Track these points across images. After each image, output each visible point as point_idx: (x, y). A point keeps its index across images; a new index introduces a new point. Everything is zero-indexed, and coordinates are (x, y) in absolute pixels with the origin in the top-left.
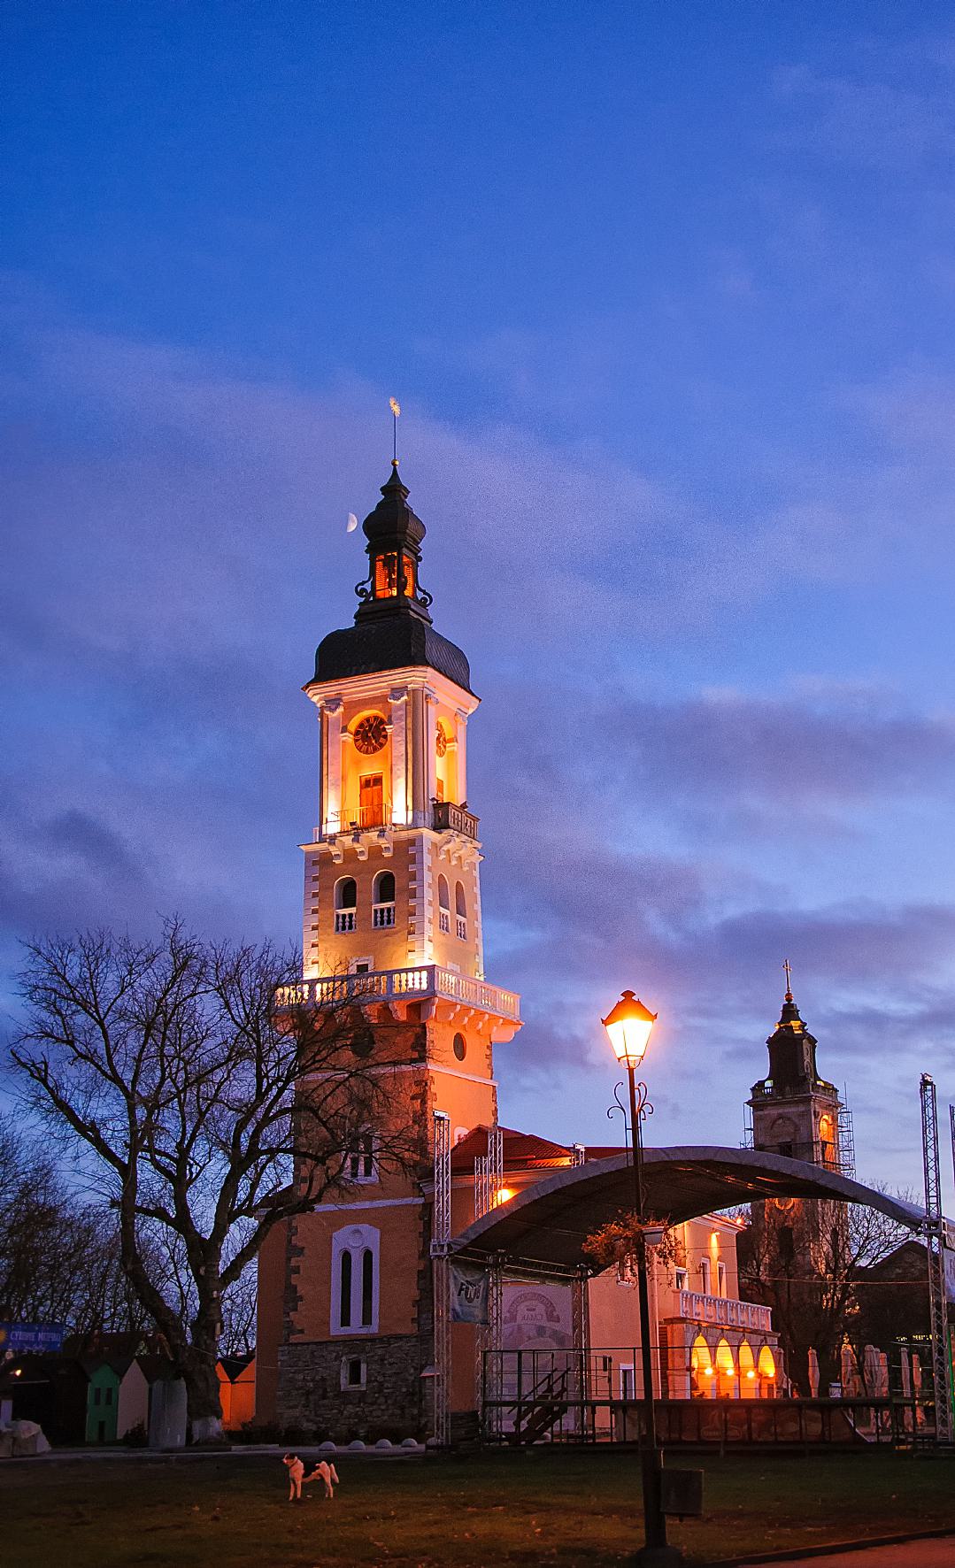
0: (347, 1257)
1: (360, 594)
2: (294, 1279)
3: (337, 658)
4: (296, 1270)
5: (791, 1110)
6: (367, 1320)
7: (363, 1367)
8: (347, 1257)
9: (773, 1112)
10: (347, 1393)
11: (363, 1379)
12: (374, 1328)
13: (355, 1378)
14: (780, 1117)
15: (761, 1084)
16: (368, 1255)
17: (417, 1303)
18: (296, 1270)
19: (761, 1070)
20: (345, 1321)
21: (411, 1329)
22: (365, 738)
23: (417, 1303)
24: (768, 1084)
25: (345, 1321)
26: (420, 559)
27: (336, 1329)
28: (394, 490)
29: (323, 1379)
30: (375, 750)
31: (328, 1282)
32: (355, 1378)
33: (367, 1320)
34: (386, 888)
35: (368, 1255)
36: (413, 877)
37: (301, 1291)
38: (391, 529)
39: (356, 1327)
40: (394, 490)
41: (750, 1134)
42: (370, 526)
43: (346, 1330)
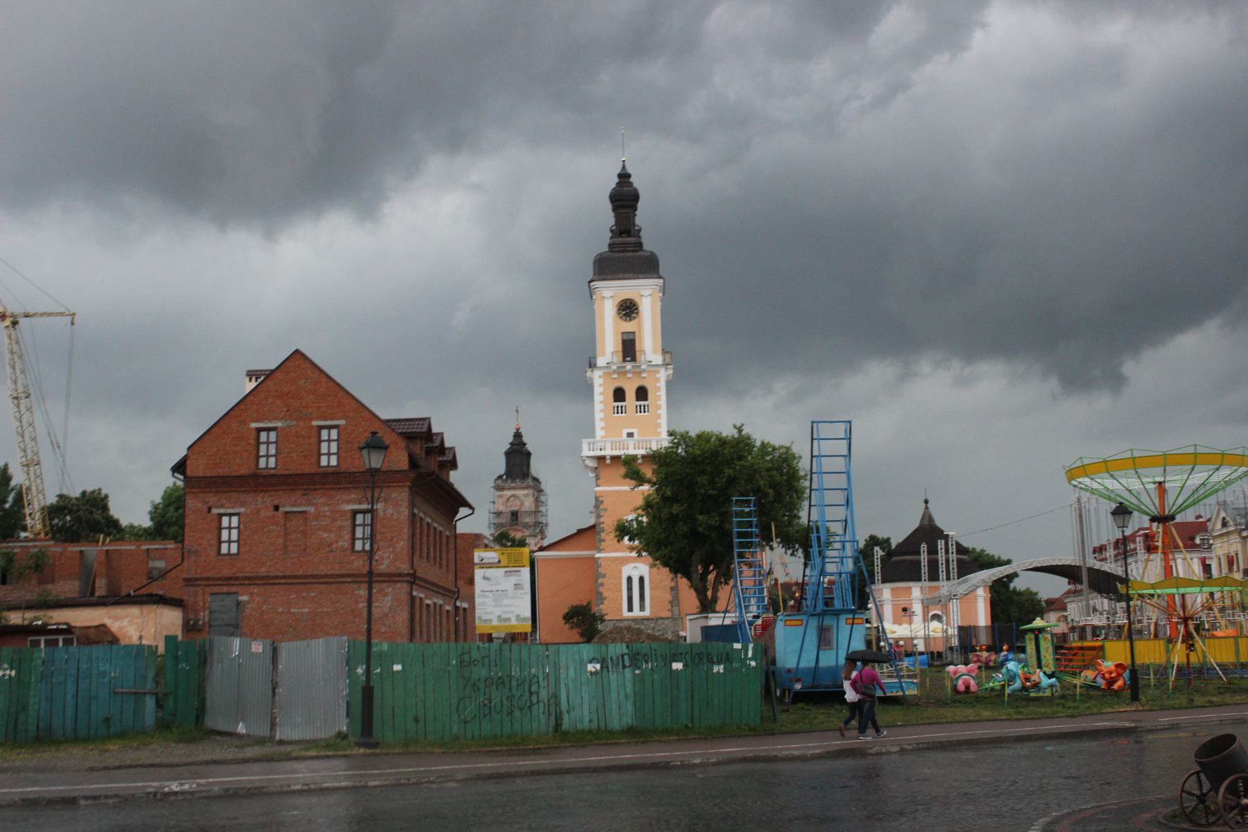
0: (630, 579)
2: (601, 589)
4: (602, 585)
6: (642, 608)
8: (630, 579)
9: (509, 493)
12: (647, 613)
16: (641, 579)
17: (671, 602)
18: (602, 585)
20: (630, 609)
21: (669, 614)
23: (671, 602)
25: (630, 609)
27: (626, 614)
31: (620, 591)
33: (642, 608)
34: (642, 393)
35: (641, 579)
37: (605, 594)
39: (636, 613)
43: (630, 614)
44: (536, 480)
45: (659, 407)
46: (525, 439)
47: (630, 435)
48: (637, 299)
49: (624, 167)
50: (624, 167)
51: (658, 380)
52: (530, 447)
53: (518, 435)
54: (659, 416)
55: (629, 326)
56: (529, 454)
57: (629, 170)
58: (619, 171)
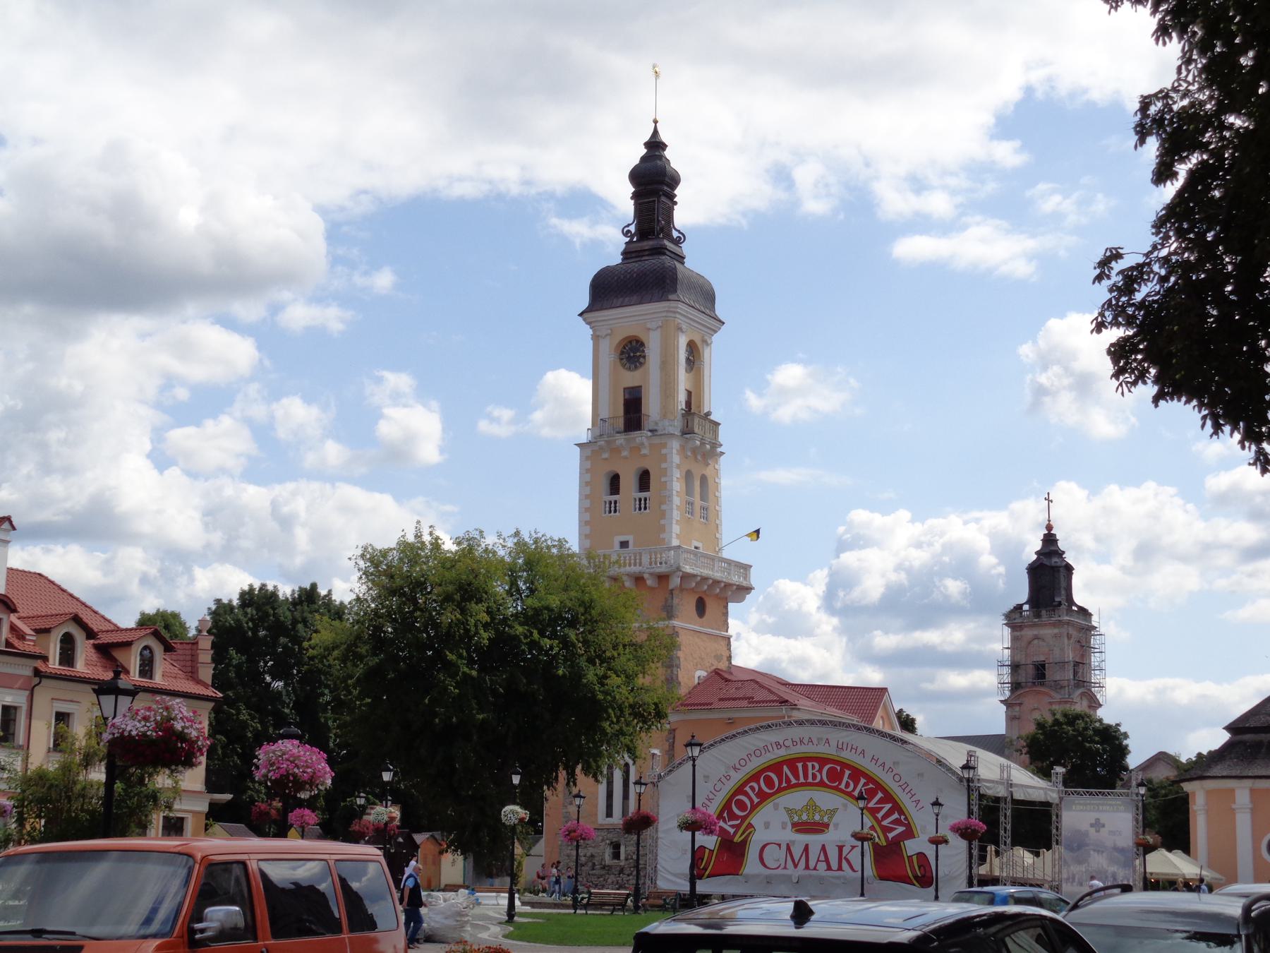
1: (626, 234)
3: (608, 290)
5: (1047, 632)
7: (622, 849)
9: (1028, 633)
10: (610, 867)
11: (623, 856)
13: (616, 855)
14: (1036, 637)
15: (1019, 608)
19: (1022, 593)
20: (609, 814)
22: (629, 358)
24: (1026, 607)
25: (609, 814)
26: (676, 203)
27: (602, 819)
28: (655, 145)
29: (592, 856)
30: (636, 368)
32: (616, 855)
34: (644, 480)
36: (664, 472)
38: (654, 181)
40: (655, 145)
41: (1007, 652)
42: (636, 176)
44: (1084, 612)
45: (665, 499)
46: (1061, 545)
47: (624, 544)
48: (643, 338)
49: (656, 132)
50: (656, 132)
51: (664, 458)
52: (1069, 558)
53: (1050, 539)
54: (663, 515)
55: (631, 378)
56: (1069, 569)
57: (664, 137)
58: (647, 138)
